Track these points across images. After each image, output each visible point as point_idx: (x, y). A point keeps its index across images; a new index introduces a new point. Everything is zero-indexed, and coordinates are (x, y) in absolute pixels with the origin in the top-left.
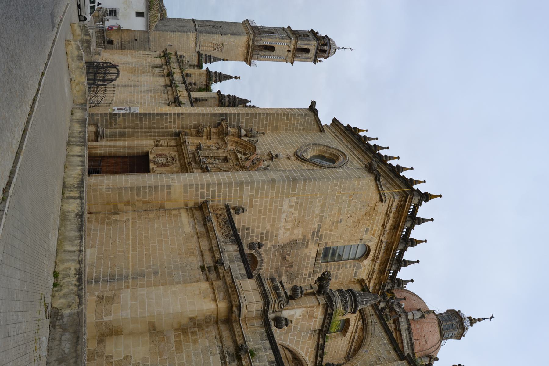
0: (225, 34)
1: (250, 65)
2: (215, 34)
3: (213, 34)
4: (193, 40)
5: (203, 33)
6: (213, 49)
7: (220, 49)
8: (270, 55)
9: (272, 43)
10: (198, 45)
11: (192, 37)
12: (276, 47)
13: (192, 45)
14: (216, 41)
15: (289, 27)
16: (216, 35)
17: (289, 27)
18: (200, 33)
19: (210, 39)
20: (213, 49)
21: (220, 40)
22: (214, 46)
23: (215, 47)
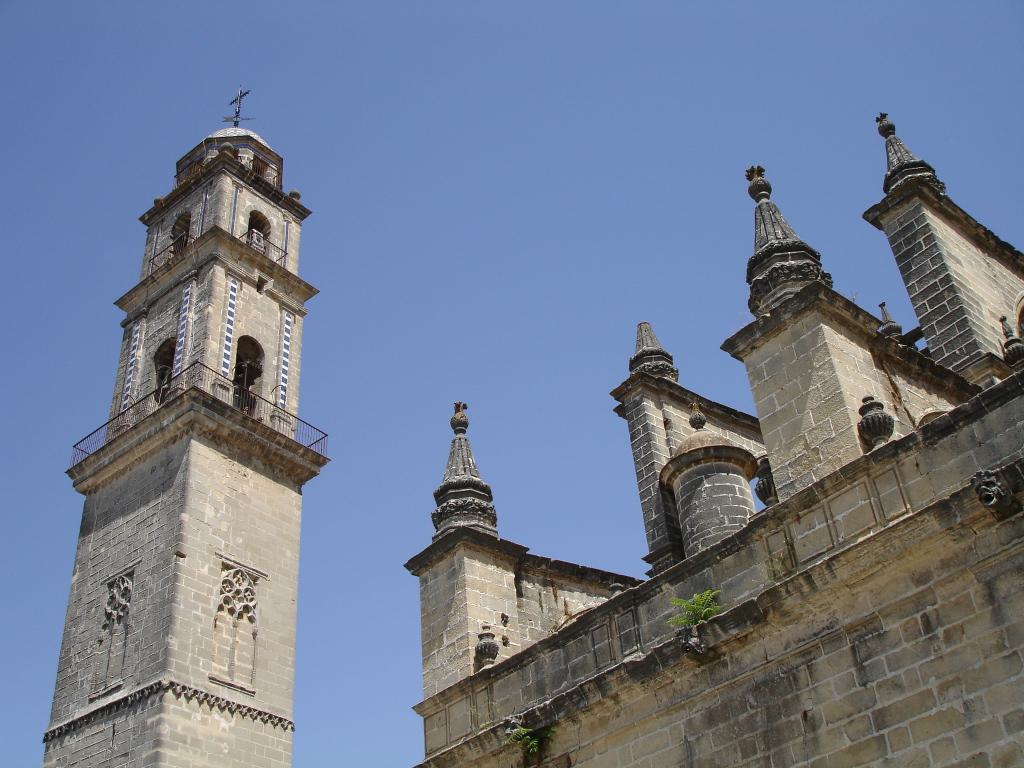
0: (179, 538)
1: (320, 461)
2: (173, 589)
3: (172, 600)
4: (199, 716)
5: (167, 652)
6: (245, 620)
7: (245, 585)
8: (278, 367)
9: (228, 339)
10: (225, 694)
11: (188, 716)
12: (241, 329)
13: (224, 724)
14: (210, 591)
15: (120, 303)
16: (182, 584)
17: (120, 303)
18: (163, 667)
19: (198, 619)
20: (245, 620)
21: (205, 571)
22: (231, 611)
23: (239, 606)
